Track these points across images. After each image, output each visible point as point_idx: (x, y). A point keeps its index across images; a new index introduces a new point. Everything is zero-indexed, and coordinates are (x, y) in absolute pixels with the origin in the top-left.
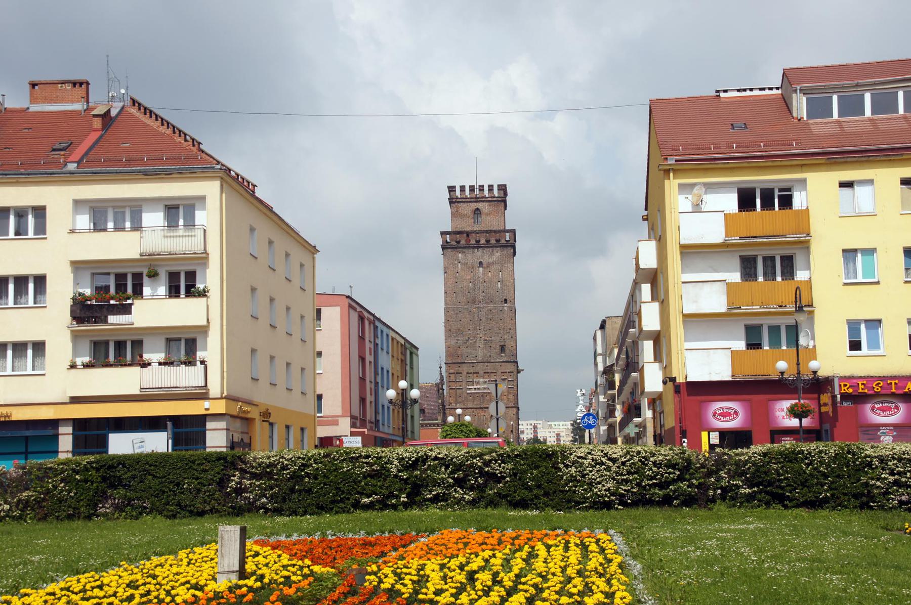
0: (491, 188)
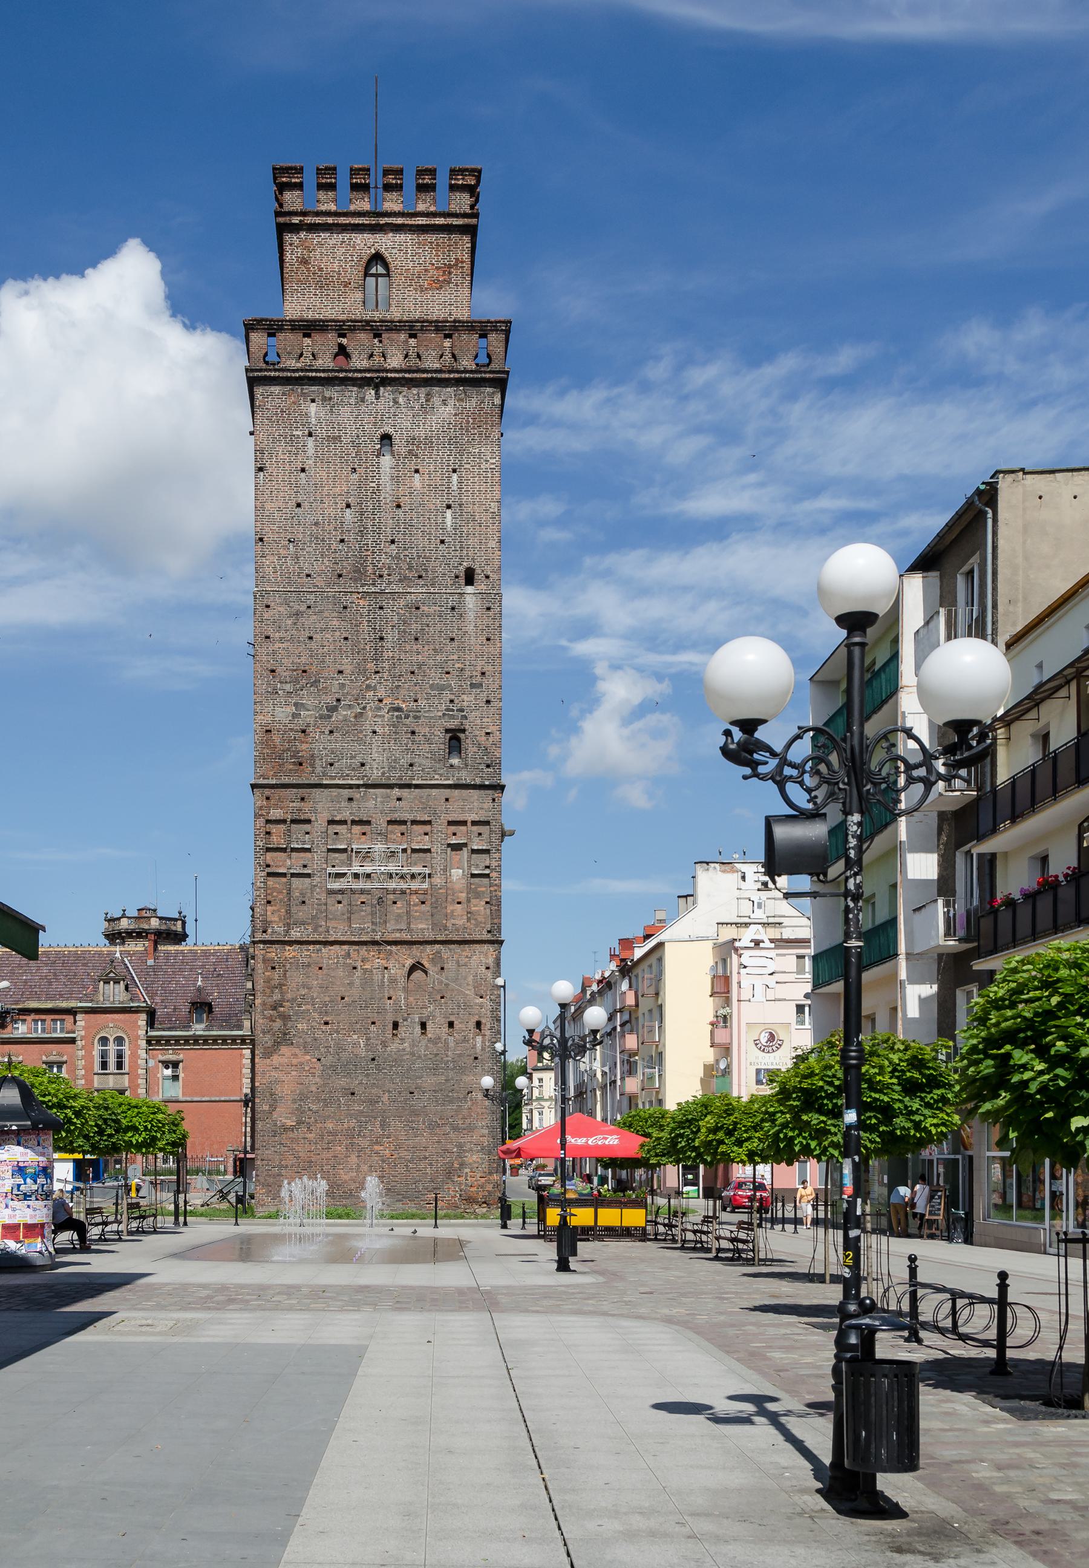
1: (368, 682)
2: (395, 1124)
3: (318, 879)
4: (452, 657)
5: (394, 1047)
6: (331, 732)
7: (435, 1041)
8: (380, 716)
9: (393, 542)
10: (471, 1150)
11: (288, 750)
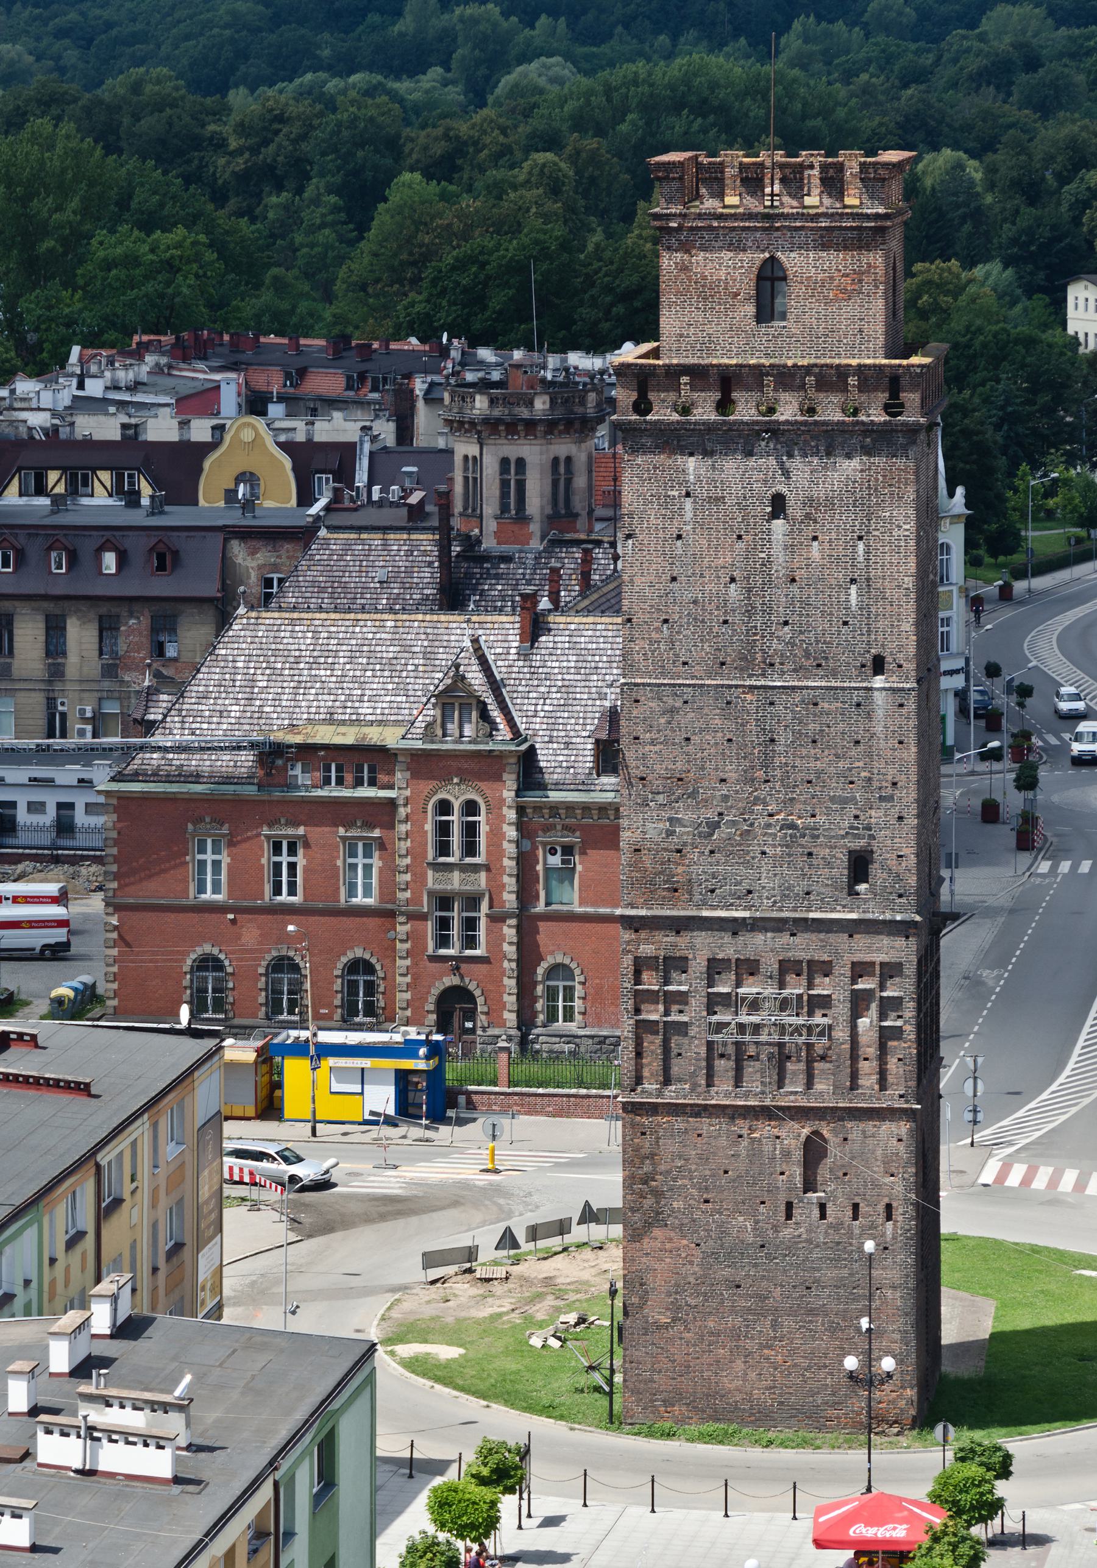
2: (788, 1323)
4: (857, 764)
5: (787, 1232)
7: (837, 1227)
9: (786, 623)
11: (661, 873)
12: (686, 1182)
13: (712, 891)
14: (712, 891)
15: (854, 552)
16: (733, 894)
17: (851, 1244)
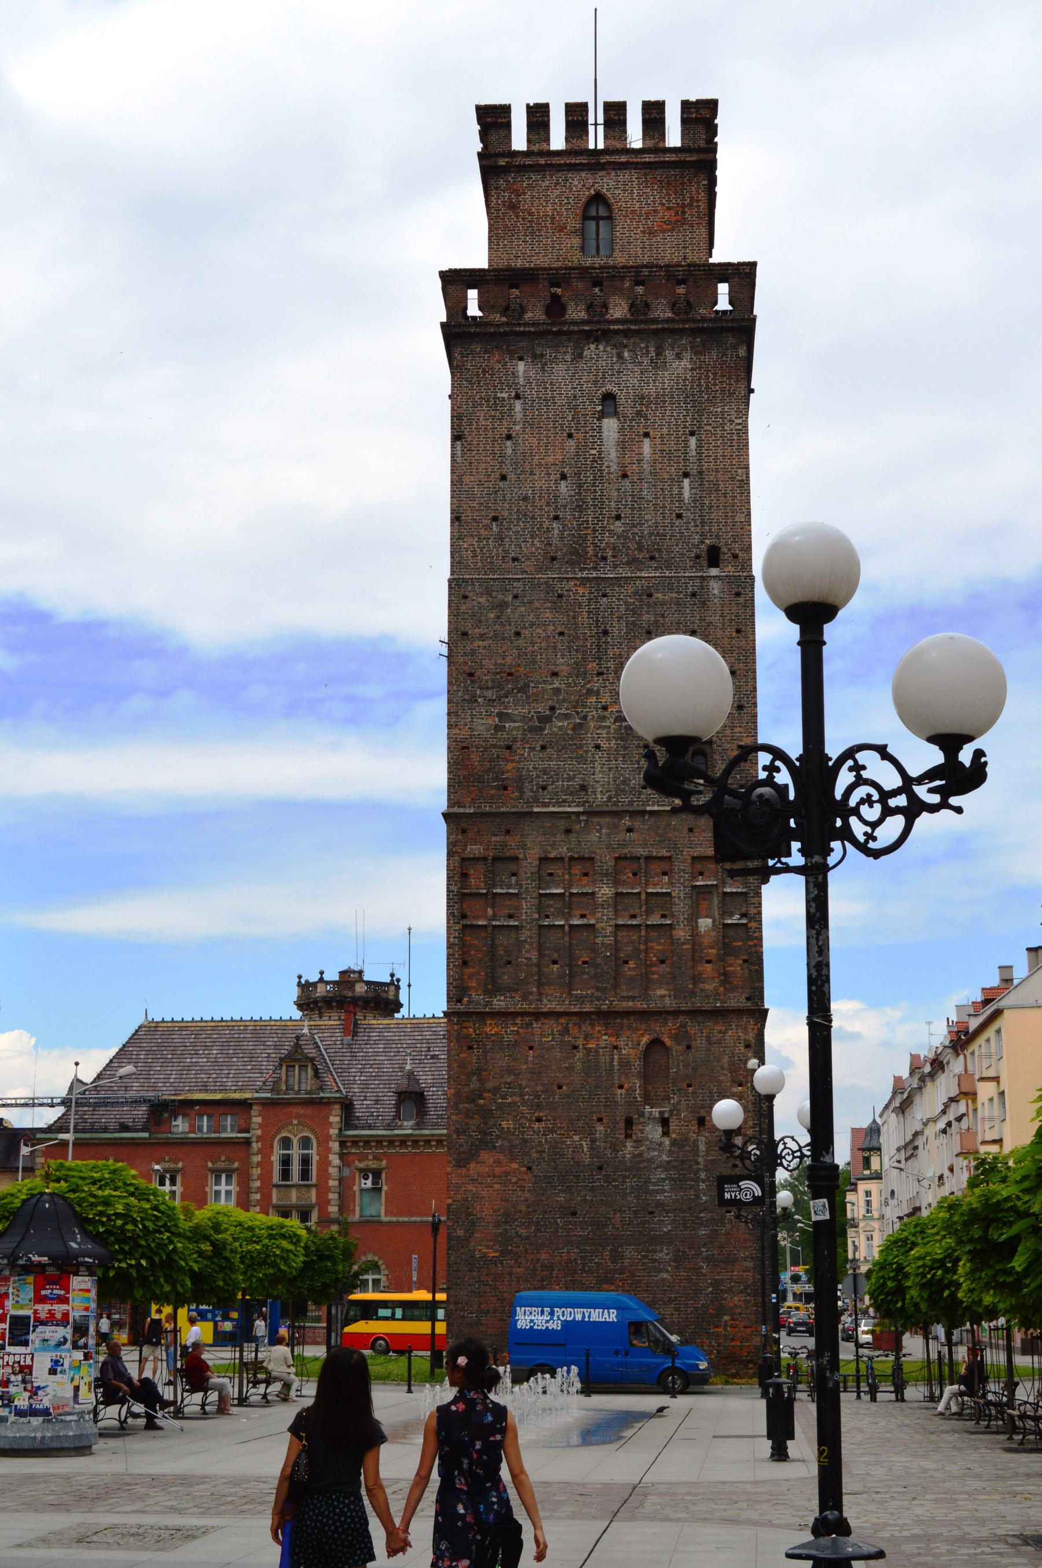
0: (654, 113)
1: (588, 686)
3: (529, 933)
6: (543, 748)
8: (605, 727)
9: (618, 517)
10: (730, 1290)
11: (489, 770)
12: (517, 1099)
13: (544, 788)
14: (544, 788)
15: (686, 446)
16: (567, 791)
17: (698, 1163)
